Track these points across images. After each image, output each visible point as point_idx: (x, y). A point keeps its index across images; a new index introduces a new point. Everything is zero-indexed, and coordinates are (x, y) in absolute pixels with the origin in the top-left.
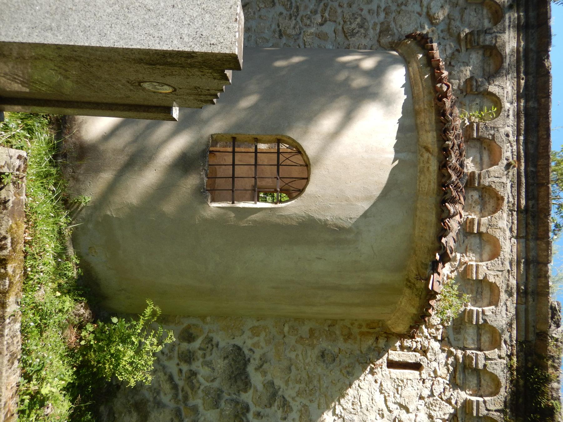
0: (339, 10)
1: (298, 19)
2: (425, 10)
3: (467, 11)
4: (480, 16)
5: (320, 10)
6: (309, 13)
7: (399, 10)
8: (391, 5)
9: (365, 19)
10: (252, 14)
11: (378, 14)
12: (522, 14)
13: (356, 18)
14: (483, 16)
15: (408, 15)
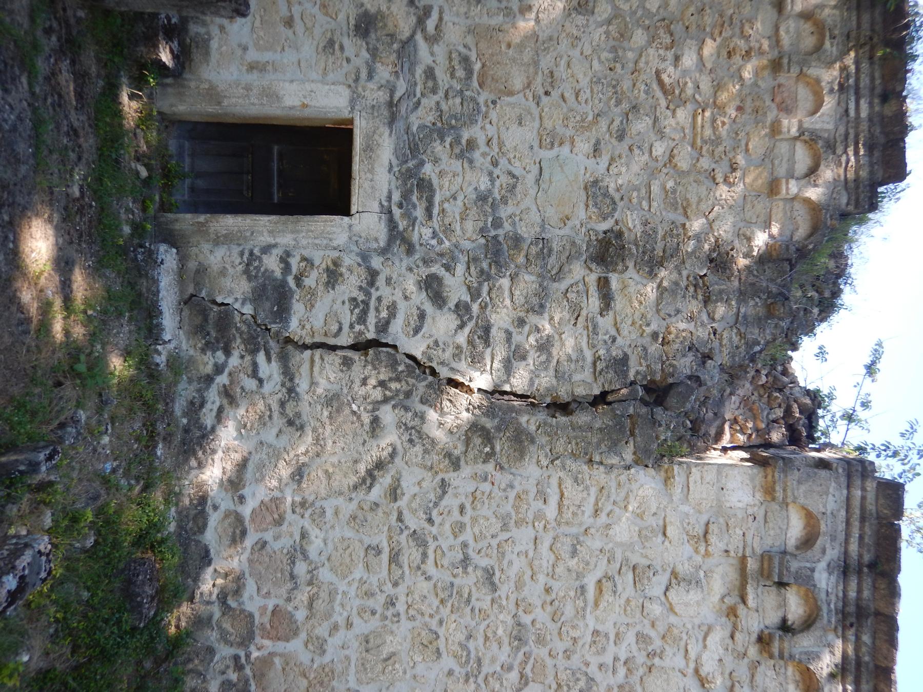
0: (549, 662)
1: (480, 680)
2: (692, 665)
3: (761, 669)
4: (781, 679)
5: (516, 664)
6: (499, 669)
7: (649, 664)
8: (636, 654)
9: (592, 679)
10: (401, 673)
11: (614, 671)
12: (849, 687)
13: (578, 679)
14: (786, 678)
15: (665, 676)
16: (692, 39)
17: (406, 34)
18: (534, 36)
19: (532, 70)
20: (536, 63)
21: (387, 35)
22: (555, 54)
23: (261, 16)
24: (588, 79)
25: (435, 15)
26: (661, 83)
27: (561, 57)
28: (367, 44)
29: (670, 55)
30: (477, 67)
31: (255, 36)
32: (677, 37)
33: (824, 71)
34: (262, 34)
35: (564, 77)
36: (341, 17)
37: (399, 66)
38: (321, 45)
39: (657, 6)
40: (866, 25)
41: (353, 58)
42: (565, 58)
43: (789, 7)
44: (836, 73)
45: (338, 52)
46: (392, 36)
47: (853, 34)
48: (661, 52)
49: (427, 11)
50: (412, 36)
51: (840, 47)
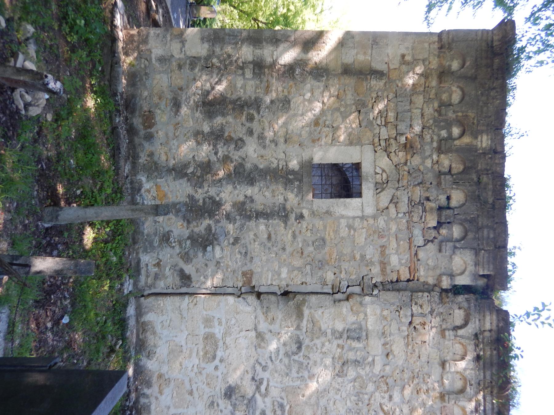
16: (398, 386)
17: (251, 395)
18: (317, 391)
19: (315, 407)
20: (317, 404)
21: (241, 397)
22: (327, 398)
23: (176, 391)
24: (345, 410)
25: (265, 383)
26: (382, 410)
27: (330, 400)
28: (231, 402)
29: (387, 396)
30: (287, 408)
31: (173, 401)
32: (390, 385)
33: (467, 403)
34: (177, 400)
35: (332, 409)
36: (218, 389)
37: (247, 412)
38: (207, 405)
39: (379, 370)
40: (488, 377)
41: (224, 409)
42: (333, 400)
43: (448, 370)
44: (473, 404)
45: (216, 408)
46: (243, 397)
47: (482, 383)
48: (382, 394)
49: (261, 382)
50: (253, 396)
51: (475, 389)
